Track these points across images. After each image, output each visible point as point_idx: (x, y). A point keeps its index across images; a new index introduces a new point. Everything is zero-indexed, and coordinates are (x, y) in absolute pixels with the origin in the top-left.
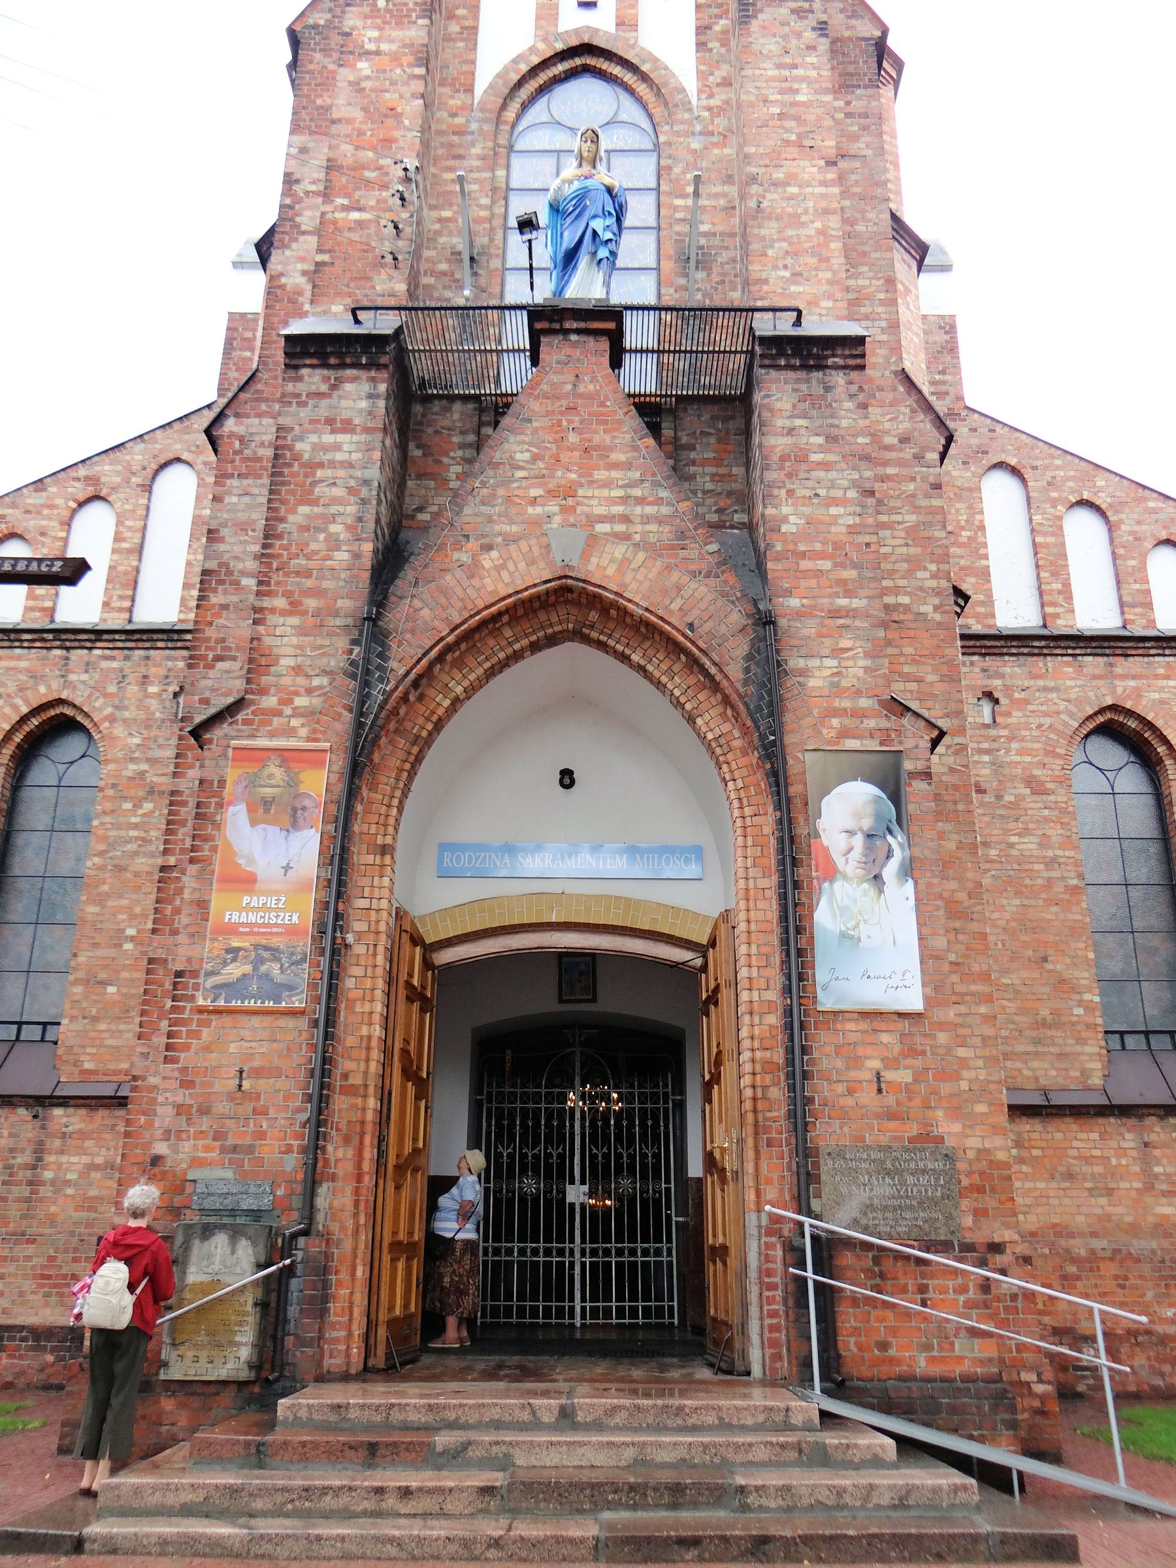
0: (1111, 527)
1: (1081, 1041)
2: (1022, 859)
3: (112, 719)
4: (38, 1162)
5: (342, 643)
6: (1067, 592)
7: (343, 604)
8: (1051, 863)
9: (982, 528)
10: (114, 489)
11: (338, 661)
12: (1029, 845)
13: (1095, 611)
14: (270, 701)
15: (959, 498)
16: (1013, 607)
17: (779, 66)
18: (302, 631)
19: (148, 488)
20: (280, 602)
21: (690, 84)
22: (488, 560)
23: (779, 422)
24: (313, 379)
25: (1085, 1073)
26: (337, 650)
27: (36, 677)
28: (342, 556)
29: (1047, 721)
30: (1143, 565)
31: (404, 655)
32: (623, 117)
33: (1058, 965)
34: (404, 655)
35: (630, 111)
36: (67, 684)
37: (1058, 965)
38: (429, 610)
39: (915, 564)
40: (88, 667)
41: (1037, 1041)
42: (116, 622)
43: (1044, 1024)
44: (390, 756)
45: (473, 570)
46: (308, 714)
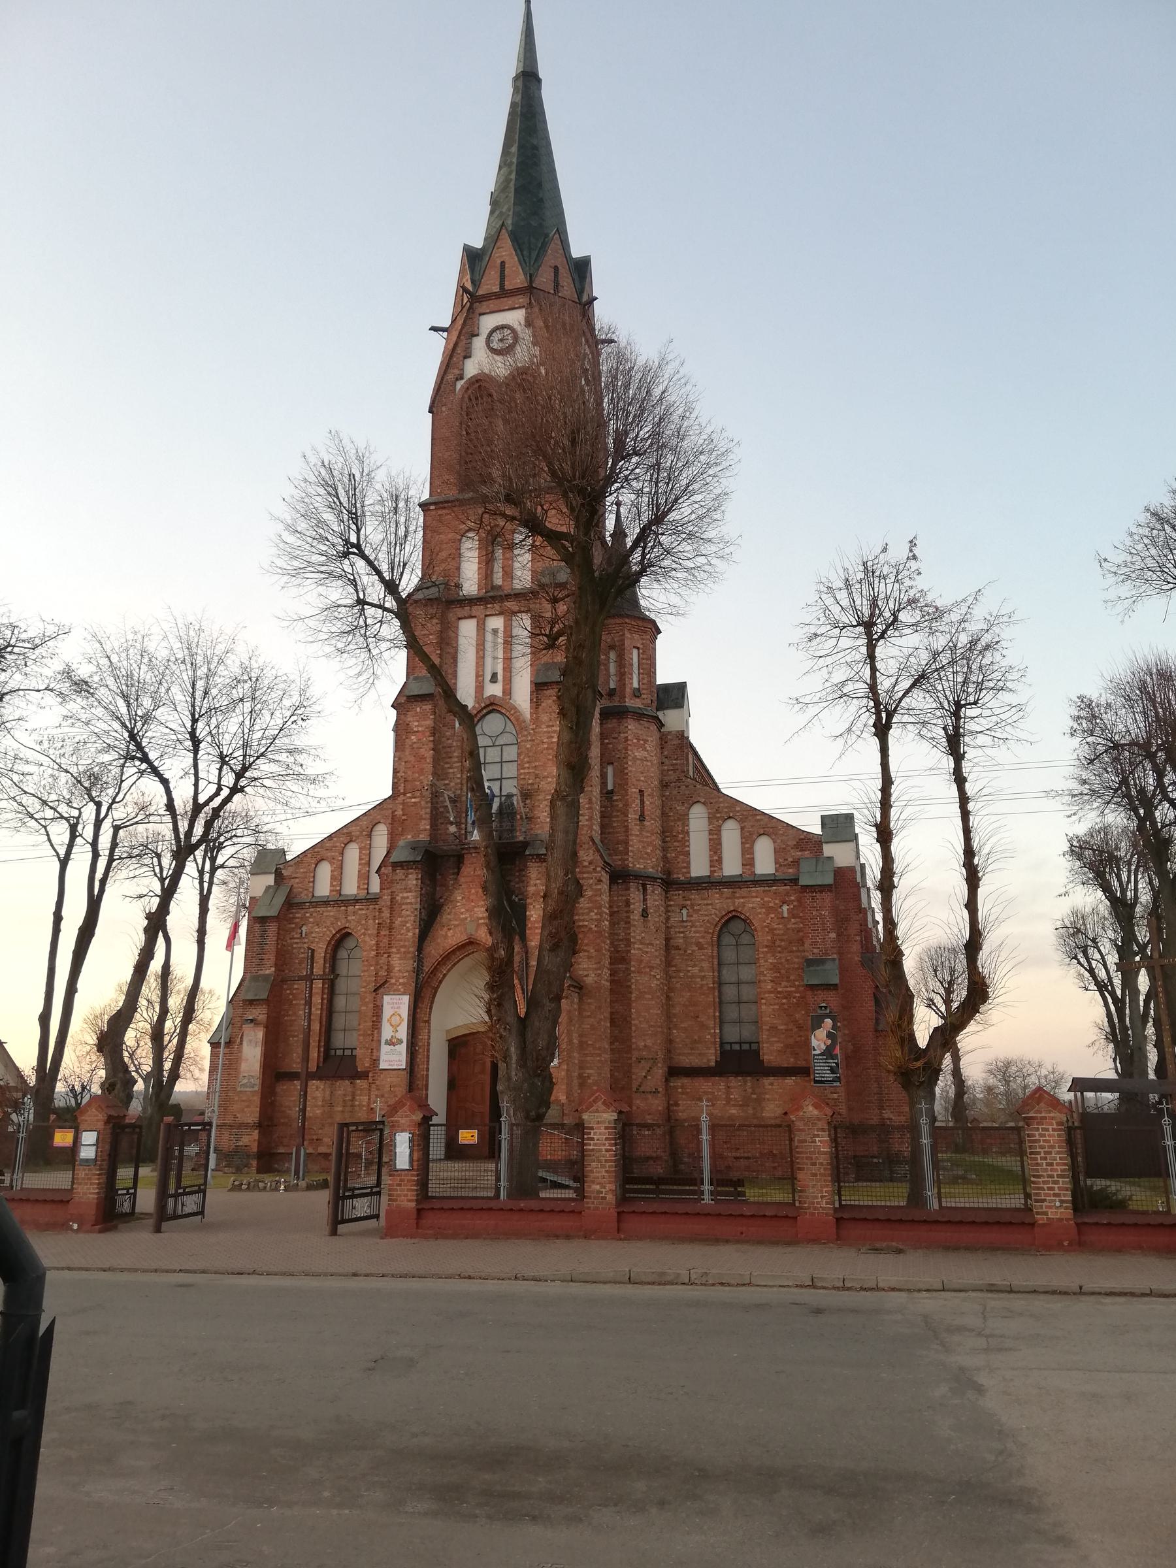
0: (742, 829)
1: (708, 1048)
2: (693, 977)
3: (364, 934)
4: (353, 1099)
5: (411, 962)
6: (720, 860)
7: (411, 949)
8: (703, 978)
9: (688, 833)
10: (358, 837)
11: (410, 968)
12: (696, 970)
13: (732, 867)
14: (393, 981)
15: (679, 820)
16: (699, 867)
17: (548, 726)
18: (400, 959)
19: (370, 836)
20: (394, 950)
21: (528, 716)
22: (450, 933)
23: (532, 882)
24: (400, 873)
25: (709, 1060)
26: (410, 964)
27: (337, 919)
28: (410, 934)
29: (706, 918)
30: (752, 847)
31: (427, 967)
32: (508, 729)
33: (703, 1018)
34: (427, 967)
35: (510, 727)
36: (348, 921)
37: (703, 1018)
38: (434, 951)
39: (590, 910)
40: (354, 913)
41: (692, 1049)
42: (363, 894)
43: (695, 1042)
44: (427, 993)
45: (446, 937)
46: (403, 984)
